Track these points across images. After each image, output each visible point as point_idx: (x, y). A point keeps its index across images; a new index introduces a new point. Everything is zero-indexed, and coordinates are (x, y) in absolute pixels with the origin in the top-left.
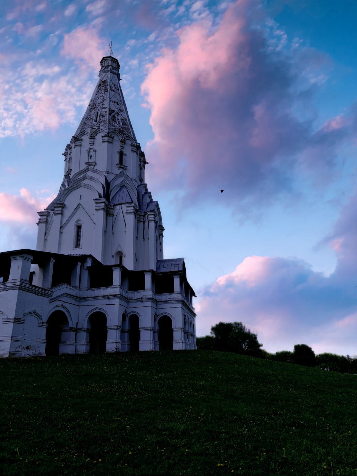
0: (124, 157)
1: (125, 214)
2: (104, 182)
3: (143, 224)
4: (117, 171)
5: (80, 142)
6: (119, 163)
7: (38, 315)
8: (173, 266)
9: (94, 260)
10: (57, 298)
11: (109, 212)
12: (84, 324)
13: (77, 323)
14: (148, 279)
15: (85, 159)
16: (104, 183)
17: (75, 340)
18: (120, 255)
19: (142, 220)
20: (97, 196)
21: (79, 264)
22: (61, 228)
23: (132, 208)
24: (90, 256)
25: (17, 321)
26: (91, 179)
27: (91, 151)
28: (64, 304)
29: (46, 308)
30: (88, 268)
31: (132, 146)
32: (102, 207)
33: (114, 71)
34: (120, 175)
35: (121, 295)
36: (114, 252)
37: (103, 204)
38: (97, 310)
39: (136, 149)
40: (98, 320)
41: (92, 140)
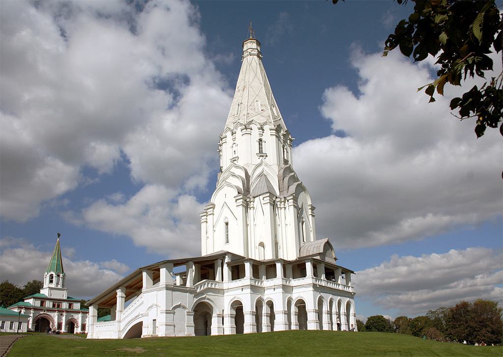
0: (263, 144)
1: (263, 205)
2: (244, 176)
3: (285, 210)
4: (258, 161)
5: (225, 139)
6: (259, 152)
7: (184, 308)
8: (315, 249)
9: (233, 256)
10: (202, 293)
11: (247, 206)
12: (228, 311)
13: (223, 310)
14: (279, 266)
15: (231, 155)
16: (244, 176)
17: (223, 324)
18: (262, 245)
19: (282, 206)
20: (236, 194)
21: (220, 262)
22: (214, 227)
23: (268, 198)
24: (228, 253)
25: (167, 312)
26: (234, 175)
27: (234, 145)
28: (208, 297)
29: (189, 301)
30: (228, 264)
31: (271, 130)
32: (241, 203)
33: (253, 52)
34: (260, 165)
35: (251, 285)
36: (257, 245)
37: (241, 200)
38: (236, 299)
39: (274, 131)
40: (238, 308)
41: (234, 135)
